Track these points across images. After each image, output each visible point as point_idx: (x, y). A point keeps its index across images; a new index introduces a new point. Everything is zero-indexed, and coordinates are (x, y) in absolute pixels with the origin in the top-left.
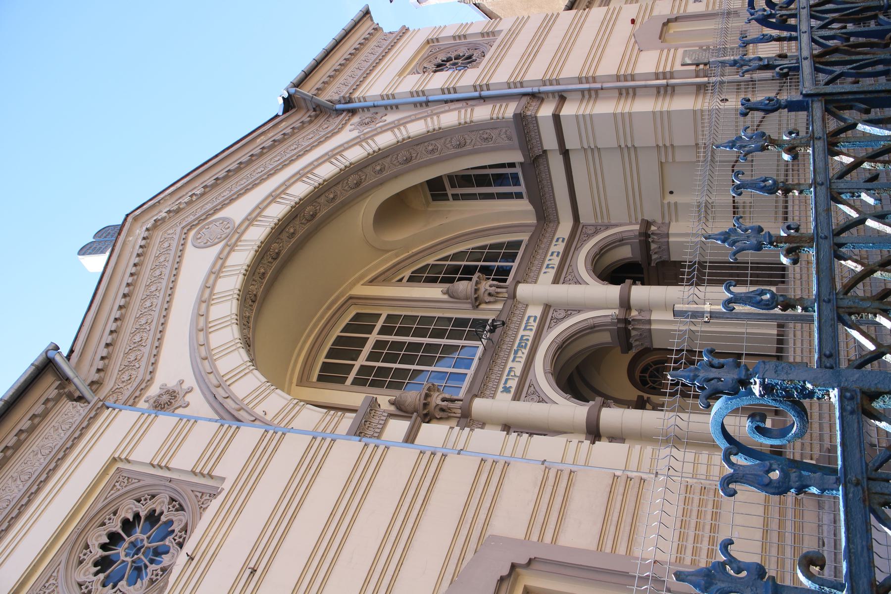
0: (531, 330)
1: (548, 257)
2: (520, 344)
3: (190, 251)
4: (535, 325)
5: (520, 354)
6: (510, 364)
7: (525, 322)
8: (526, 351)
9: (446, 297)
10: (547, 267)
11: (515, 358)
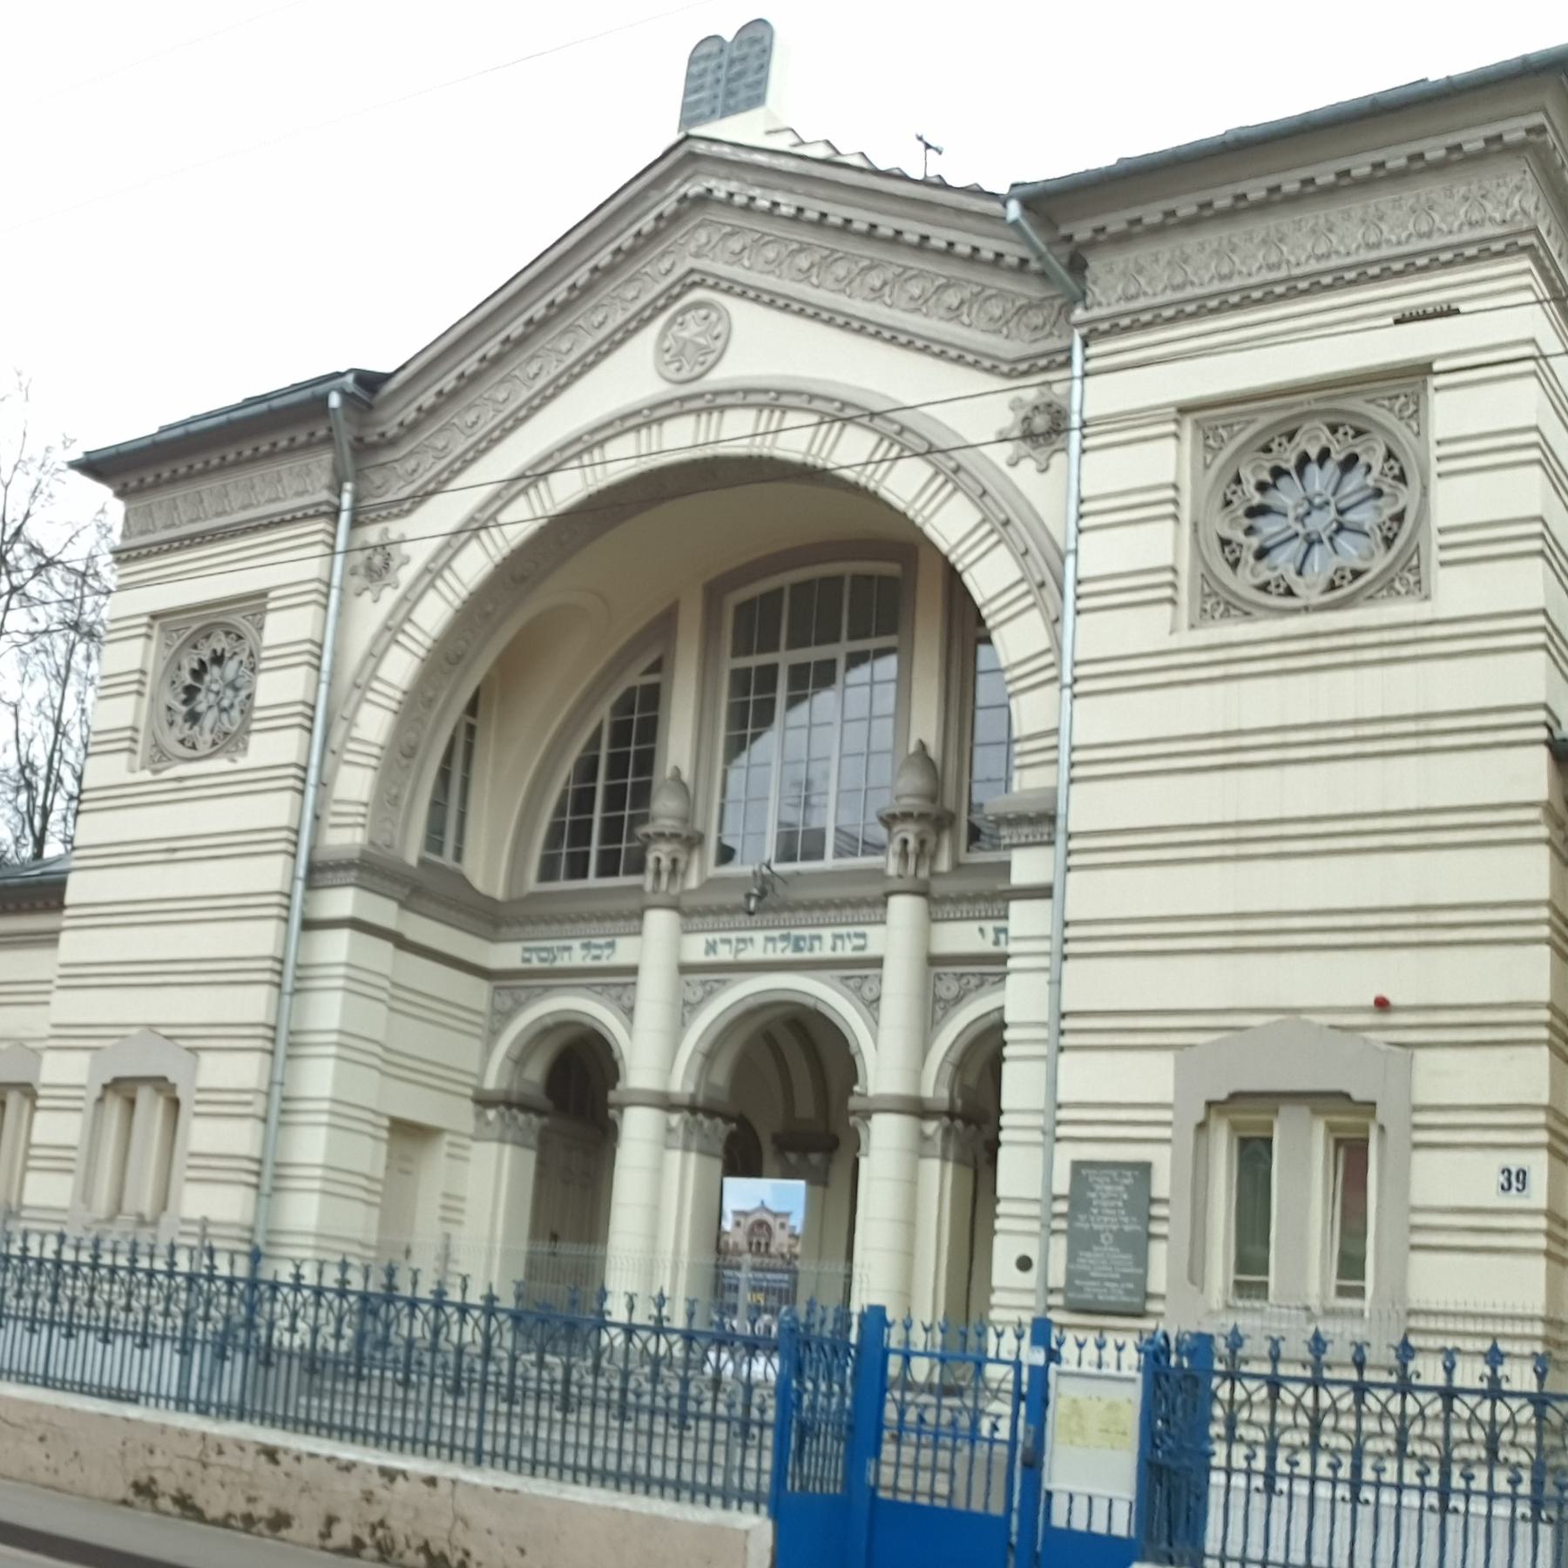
0: (834, 948)
2: (803, 938)
4: (846, 951)
5: (781, 945)
6: (759, 936)
8: (789, 955)
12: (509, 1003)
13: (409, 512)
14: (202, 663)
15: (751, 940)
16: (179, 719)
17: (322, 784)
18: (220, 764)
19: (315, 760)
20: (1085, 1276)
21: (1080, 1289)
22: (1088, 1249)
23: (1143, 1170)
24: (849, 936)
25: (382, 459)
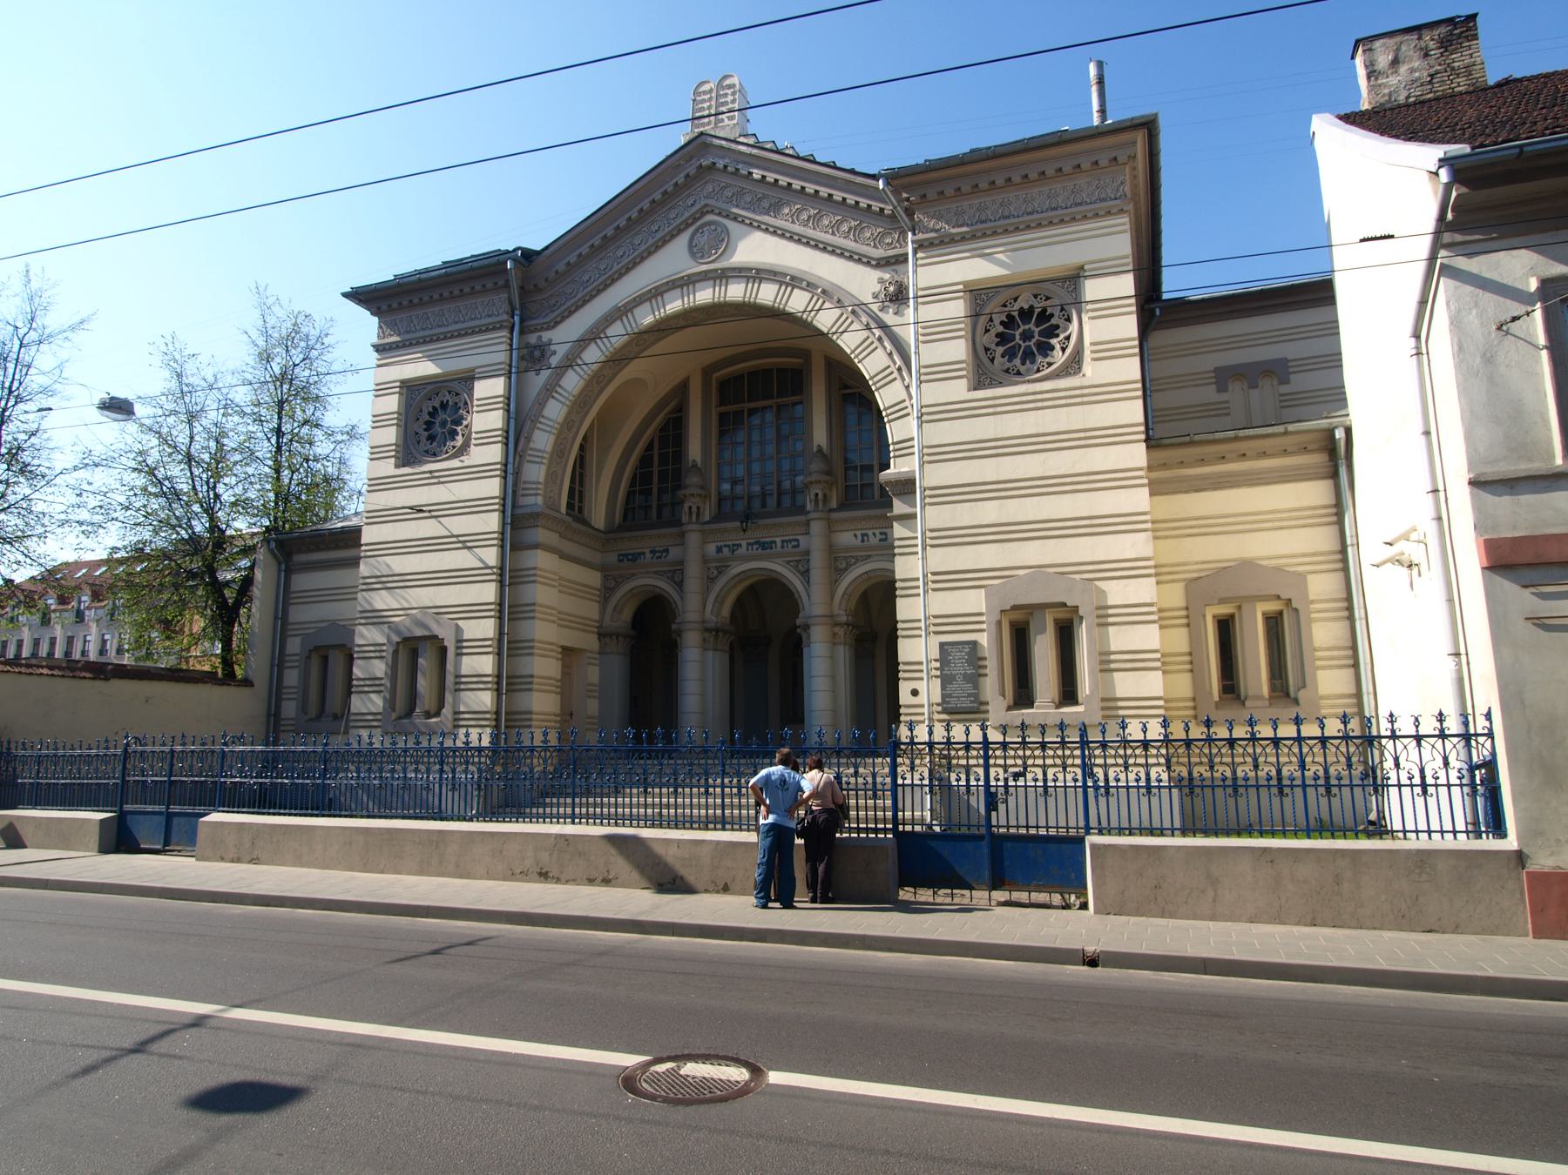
0: (783, 547)
1: (877, 532)
3: (682, 241)
5: (755, 547)
7: (791, 537)
9: (815, 450)
10: (863, 535)
11: (752, 544)
12: (613, 584)
13: (554, 327)
14: (434, 408)
15: (740, 545)
16: (423, 439)
17: (517, 473)
18: (455, 463)
19: (511, 459)
20: (950, 696)
21: (948, 703)
22: (951, 683)
23: (974, 644)
24: (790, 541)
25: (534, 299)
